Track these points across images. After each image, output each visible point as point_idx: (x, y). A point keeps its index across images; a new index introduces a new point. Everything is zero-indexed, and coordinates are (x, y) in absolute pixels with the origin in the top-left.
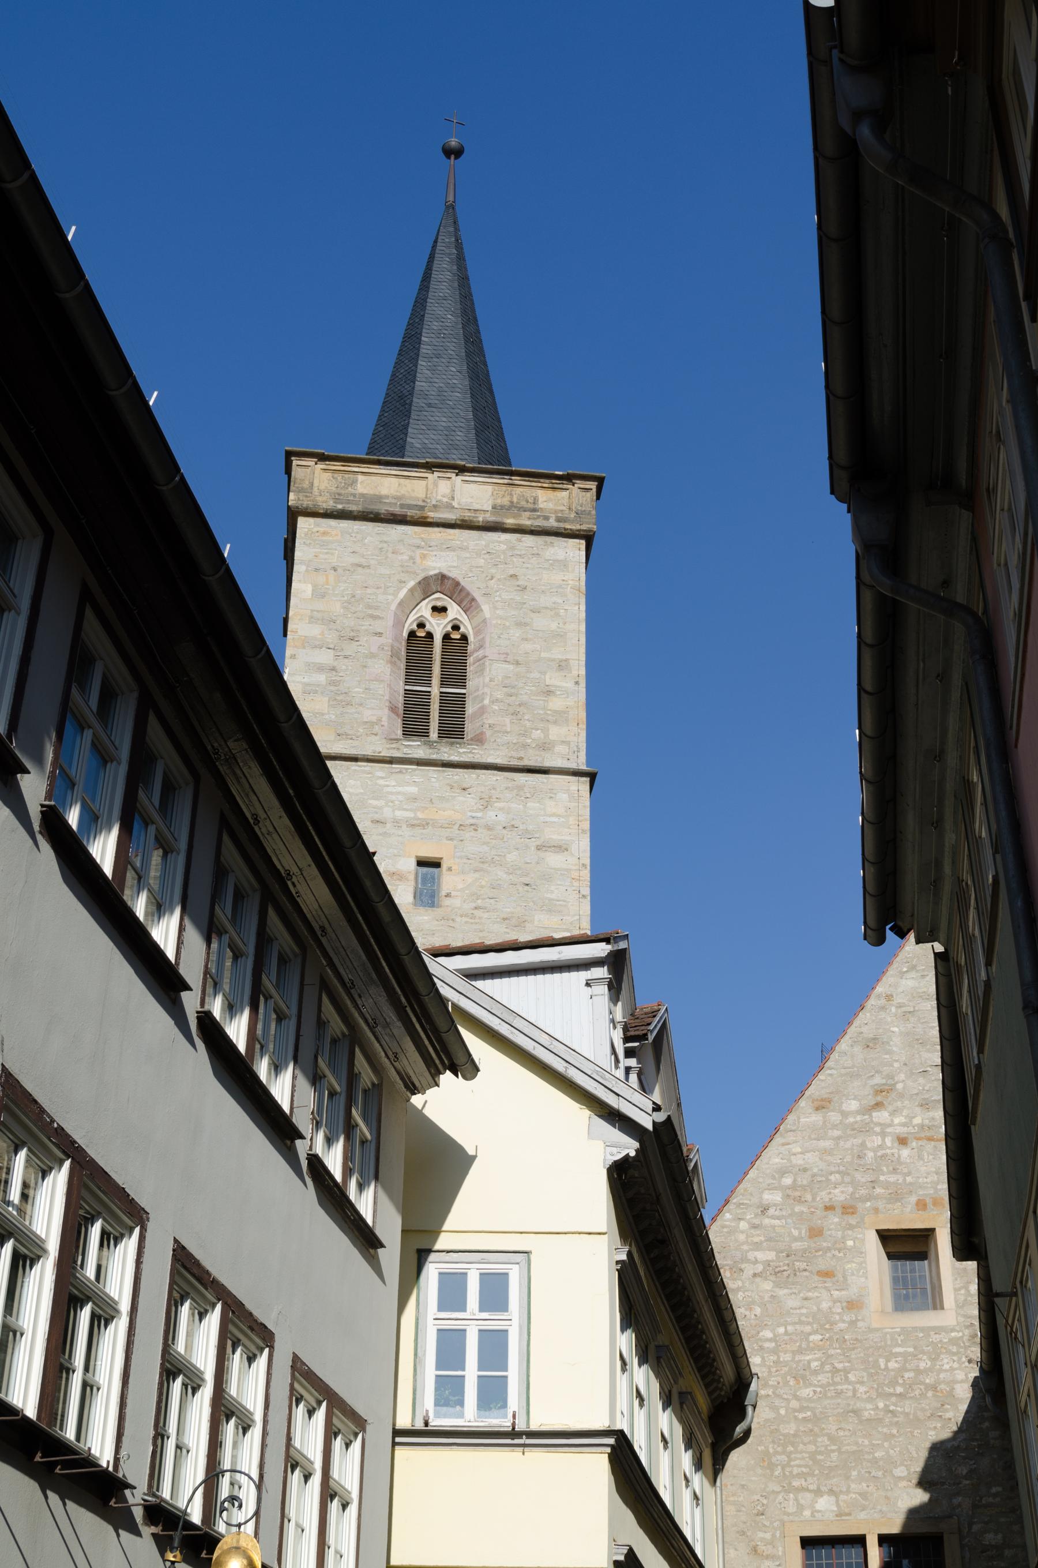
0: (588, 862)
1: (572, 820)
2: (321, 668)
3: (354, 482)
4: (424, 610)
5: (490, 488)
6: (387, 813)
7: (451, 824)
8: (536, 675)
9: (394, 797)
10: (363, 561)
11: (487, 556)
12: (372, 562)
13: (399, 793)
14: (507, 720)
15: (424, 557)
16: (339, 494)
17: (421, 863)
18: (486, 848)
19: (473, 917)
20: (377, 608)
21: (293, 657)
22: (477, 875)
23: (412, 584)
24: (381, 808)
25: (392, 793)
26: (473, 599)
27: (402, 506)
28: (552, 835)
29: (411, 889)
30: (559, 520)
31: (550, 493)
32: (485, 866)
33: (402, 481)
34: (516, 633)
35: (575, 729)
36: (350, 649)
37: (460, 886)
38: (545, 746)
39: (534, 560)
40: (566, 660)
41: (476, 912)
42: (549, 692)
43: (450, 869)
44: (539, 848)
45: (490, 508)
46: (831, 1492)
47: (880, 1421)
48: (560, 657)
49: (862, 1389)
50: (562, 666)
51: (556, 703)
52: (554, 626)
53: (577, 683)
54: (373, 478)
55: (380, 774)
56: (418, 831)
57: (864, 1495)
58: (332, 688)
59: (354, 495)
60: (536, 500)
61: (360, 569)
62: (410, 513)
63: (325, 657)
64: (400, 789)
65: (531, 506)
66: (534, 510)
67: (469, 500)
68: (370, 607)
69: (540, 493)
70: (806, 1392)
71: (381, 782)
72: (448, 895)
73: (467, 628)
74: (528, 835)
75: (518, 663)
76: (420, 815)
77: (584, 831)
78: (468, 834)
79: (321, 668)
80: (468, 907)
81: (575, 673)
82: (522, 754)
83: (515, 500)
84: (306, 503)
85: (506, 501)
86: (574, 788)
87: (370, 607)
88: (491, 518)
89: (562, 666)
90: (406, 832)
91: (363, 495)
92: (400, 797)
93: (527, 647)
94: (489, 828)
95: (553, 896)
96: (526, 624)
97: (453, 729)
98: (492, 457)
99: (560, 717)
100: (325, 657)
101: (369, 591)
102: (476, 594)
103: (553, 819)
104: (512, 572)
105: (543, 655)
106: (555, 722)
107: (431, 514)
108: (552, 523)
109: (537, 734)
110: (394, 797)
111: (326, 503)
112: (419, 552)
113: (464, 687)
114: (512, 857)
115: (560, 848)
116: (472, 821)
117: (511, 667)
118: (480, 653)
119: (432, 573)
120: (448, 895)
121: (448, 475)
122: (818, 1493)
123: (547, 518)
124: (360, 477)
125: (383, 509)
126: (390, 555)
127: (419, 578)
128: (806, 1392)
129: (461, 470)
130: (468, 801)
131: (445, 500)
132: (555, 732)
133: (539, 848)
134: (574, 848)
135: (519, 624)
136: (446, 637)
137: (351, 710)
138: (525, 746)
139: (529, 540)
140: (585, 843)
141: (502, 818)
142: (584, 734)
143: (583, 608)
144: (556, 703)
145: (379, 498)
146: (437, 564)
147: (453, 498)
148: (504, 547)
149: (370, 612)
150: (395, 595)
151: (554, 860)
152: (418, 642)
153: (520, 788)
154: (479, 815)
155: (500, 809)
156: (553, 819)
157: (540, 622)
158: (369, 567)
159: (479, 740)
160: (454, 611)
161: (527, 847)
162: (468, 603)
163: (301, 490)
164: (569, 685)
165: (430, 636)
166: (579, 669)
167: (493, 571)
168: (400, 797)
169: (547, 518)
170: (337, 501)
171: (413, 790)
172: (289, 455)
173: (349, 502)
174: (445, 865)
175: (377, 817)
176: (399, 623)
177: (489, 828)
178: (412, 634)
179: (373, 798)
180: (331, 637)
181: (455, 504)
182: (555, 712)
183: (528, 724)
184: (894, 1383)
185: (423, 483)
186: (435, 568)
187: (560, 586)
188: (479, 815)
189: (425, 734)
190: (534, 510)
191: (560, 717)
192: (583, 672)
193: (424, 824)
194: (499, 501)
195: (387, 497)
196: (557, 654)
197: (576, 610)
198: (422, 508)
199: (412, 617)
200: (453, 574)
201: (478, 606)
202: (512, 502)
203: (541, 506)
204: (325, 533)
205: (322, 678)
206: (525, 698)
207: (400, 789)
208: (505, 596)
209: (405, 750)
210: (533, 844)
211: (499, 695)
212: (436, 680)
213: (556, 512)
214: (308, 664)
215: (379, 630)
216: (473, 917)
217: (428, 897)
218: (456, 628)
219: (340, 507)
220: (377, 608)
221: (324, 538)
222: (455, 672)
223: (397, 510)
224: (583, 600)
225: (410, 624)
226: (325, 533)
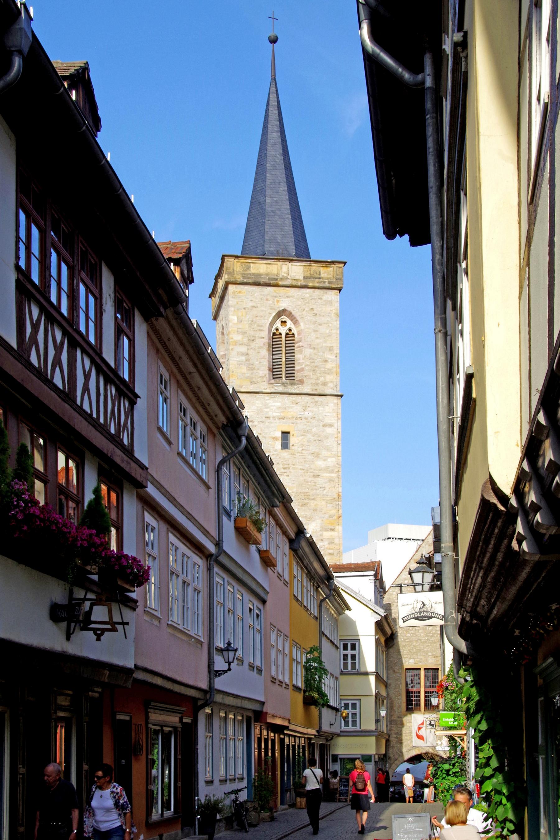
0: (340, 430)
1: (335, 414)
2: (243, 354)
3: (249, 267)
4: (278, 324)
5: (302, 267)
6: (270, 414)
7: (292, 418)
8: (321, 354)
9: (272, 408)
10: (254, 304)
11: (302, 300)
12: (259, 305)
13: (274, 406)
14: (311, 373)
15: (278, 301)
16: (244, 274)
17: (283, 433)
18: (305, 427)
19: (302, 453)
20: (262, 326)
21: (232, 349)
22: (302, 437)
23: (274, 314)
24: (268, 412)
25: (272, 406)
26: (297, 320)
27: (269, 279)
28: (328, 421)
29: (280, 443)
30: (329, 283)
31: (325, 268)
32: (305, 434)
33: (268, 266)
34: (313, 335)
35: (336, 376)
36: (253, 345)
37: (297, 442)
38: (325, 384)
39: (319, 301)
40: (332, 347)
41: (303, 452)
42: (326, 361)
43: (293, 435)
44: (323, 426)
45: (302, 278)
46: (413, 658)
47: (426, 642)
48: (330, 345)
49: (422, 634)
50: (331, 349)
51: (329, 366)
52: (327, 331)
53: (336, 356)
54: (257, 265)
55: (267, 398)
56: (282, 421)
57: (421, 659)
58: (248, 362)
59: (250, 274)
60: (320, 272)
61: (254, 309)
62: (272, 282)
63: (244, 349)
64: (274, 404)
65: (318, 276)
66: (320, 278)
67: (295, 274)
68: (258, 326)
69: (321, 269)
70: (408, 635)
71: (268, 402)
72: (293, 445)
73: (294, 331)
74: (319, 421)
75: (314, 349)
76: (282, 414)
77: (339, 419)
78: (299, 421)
79: (243, 354)
80: (300, 449)
81: (335, 352)
82: (317, 388)
83: (312, 273)
84: (232, 279)
85: (308, 274)
86: (335, 401)
87: (258, 326)
88: (303, 283)
89: (331, 349)
90: (277, 420)
91: (253, 274)
92: (275, 408)
93: (318, 341)
94: (306, 419)
95: (329, 444)
96: (317, 331)
97: (290, 375)
98: (302, 253)
99: (329, 372)
100: (244, 349)
101: (258, 318)
102: (298, 318)
103: (328, 414)
104: (311, 307)
105: (324, 345)
106: (328, 374)
107: (281, 283)
108: (327, 285)
109: (322, 379)
110: (272, 408)
111: (240, 279)
112: (276, 299)
113: (294, 356)
114: (314, 430)
115: (331, 426)
116: (300, 416)
117: (312, 350)
118: (300, 344)
119: (281, 309)
120: (293, 445)
121: (286, 263)
122: (410, 658)
123: (324, 282)
124: (252, 265)
125: (262, 281)
126: (265, 301)
127: (277, 312)
128: (408, 635)
129: (291, 260)
130: (299, 408)
131: (285, 275)
132: (329, 378)
133: (323, 426)
134: (335, 425)
135: (315, 331)
136: (287, 334)
137: (255, 371)
138: (318, 384)
139: (317, 292)
140: (340, 423)
141: (311, 414)
142: (339, 378)
143: (338, 323)
144: (329, 366)
145: (259, 275)
146: (283, 305)
147: (288, 274)
148: (308, 295)
149: (259, 328)
150: (268, 320)
151: (329, 430)
152: (276, 335)
153: (317, 402)
154: (302, 413)
155: (310, 411)
156: (328, 414)
157: (323, 330)
158: (257, 307)
159: (301, 382)
160: (289, 324)
161: (319, 425)
162: (295, 321)
163: (229, 273)
164: (333, 357)
165: (280, 334)
166: (336, 350)
167: (304, 307)
168: (275, 408)
169: (324, 282)
170: (244, 277)
171: (279, 404)
172: (223, 257)
173: (248, 278)
174: (291, 434)
175: (267, 416)
176: (270, 331)
177: (306, 419)
178: (274, 334)
179: (266, 408)
180: (245, 340)
181: (289, 277)
182: (328, 369)
183: (319, 375)
184: (430, 633)
185: (276, 266)
186: (282, 307)
187: (329, 313)
188: (302, 413)
189: (281, 378)
190: (320, 278)
191: (329, 372)
192: (338, 352)
193: (283, 418)
194: (306, 274)
195: (263, 274)
196: (328, 344)
197: (336, 323)
198: (276, 280)
199: (274, 327)
200: (289, 309)
201: (299, 323)
202: (311, 274)
203: (322, 275)
204: (240, 292)
205: (243, 358)
206: (316, 364)
207: (274, 404)
208: (309, 318)
209: (276, 388)
210: (321, 424)
211: (308, 363)
212: (284, 355)
213: (328, 279)
214: (238, 353)
215: (263, 336)
216: (302, 453)
217: (285, 445)
218: (290, 330)
219: (245, 280)
220: (262, 326)
221: (240, 294)
222: (290, 351)
223: (267, 281)
224: (338, 319)
225: (274, 330)
226: (240, 292)
